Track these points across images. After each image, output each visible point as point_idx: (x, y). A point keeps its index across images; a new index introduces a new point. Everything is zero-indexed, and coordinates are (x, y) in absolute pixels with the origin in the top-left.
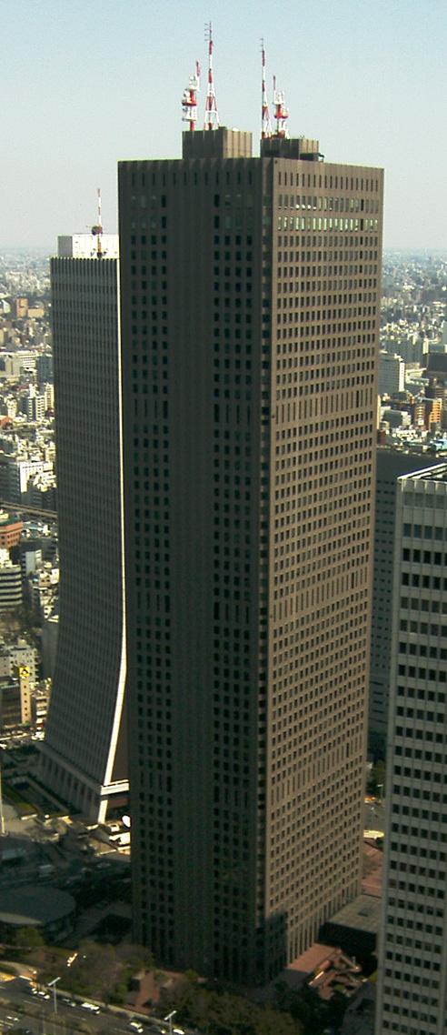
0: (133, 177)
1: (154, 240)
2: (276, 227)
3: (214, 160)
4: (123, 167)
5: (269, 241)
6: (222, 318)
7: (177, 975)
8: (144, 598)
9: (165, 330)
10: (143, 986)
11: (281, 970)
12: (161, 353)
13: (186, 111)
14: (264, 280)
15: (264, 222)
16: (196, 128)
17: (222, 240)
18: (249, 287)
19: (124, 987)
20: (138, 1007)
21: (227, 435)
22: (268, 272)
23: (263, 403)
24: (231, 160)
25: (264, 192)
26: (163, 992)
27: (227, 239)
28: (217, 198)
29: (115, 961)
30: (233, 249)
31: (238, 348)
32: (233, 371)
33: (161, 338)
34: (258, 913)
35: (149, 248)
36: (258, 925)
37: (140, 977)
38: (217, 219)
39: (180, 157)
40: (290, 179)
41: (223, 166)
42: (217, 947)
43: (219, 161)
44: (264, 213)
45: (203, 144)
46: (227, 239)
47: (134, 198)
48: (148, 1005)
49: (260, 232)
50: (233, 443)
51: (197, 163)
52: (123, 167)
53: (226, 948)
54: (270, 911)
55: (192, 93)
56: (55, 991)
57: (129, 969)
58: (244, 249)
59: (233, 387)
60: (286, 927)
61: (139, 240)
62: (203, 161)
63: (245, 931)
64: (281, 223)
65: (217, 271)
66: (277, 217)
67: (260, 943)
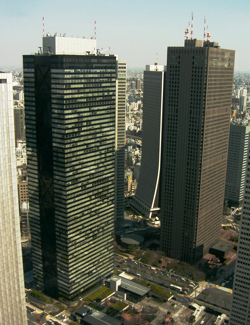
0: (172, 51)
1: (176, 67)
2: (209, 65)
3: (193, 47)
4: (169, 49)
5: (207, 68)
6: (193, 88)
7: (172, 260)
8: (168, 160)
9: (178, 90)
10: (163, 262)
11: (202, 258)
12: (177, 96)
13: (186, 34)
14: (205, 78)
15: (206, 63)
16: (188, 39)
17: (194, 68)
18: (201, 80)
19: (157, 262)
20: (161, 268)
21: (193, 118)
22: (206, 76)
23: (203, 110)
24: (197, 47)
25: (206, 56)
26: (168, 264)
27: (196, 68)
28: (193, 57)
29: (155, 255)
30: (197, 70)
31: (197, 96)
32: (196, 102)
33: (177, 92)
34: (194, 244)
35: (175, 69)
36: (194, 248)
37: (162, 260)
38: (193, 62)
39: (184, 46)
40: (213, 53)
41: (196, 48)
42: (182, 253)
43: (195, 47)
44: (206, 61)
45: (190, 43)
46: (196, 68)
47: (171, 56)
48: (164, 267)
49: (205, 66)
50: (195, 120)
51: (189, 48)
52: (169, 49)
53: (185, 254)
54: (198, 244)
55: (187, 30)
56: (140, 262)
57: (159, 258)
58: (200, 70)
59: (195, 106)
60: (203, 247)
61: (172, 67)
62: (190, 47)
63: (190, 249)
64: (210, 64)
65: (193, 75)
66: (209, 62)
67: (194, 253)
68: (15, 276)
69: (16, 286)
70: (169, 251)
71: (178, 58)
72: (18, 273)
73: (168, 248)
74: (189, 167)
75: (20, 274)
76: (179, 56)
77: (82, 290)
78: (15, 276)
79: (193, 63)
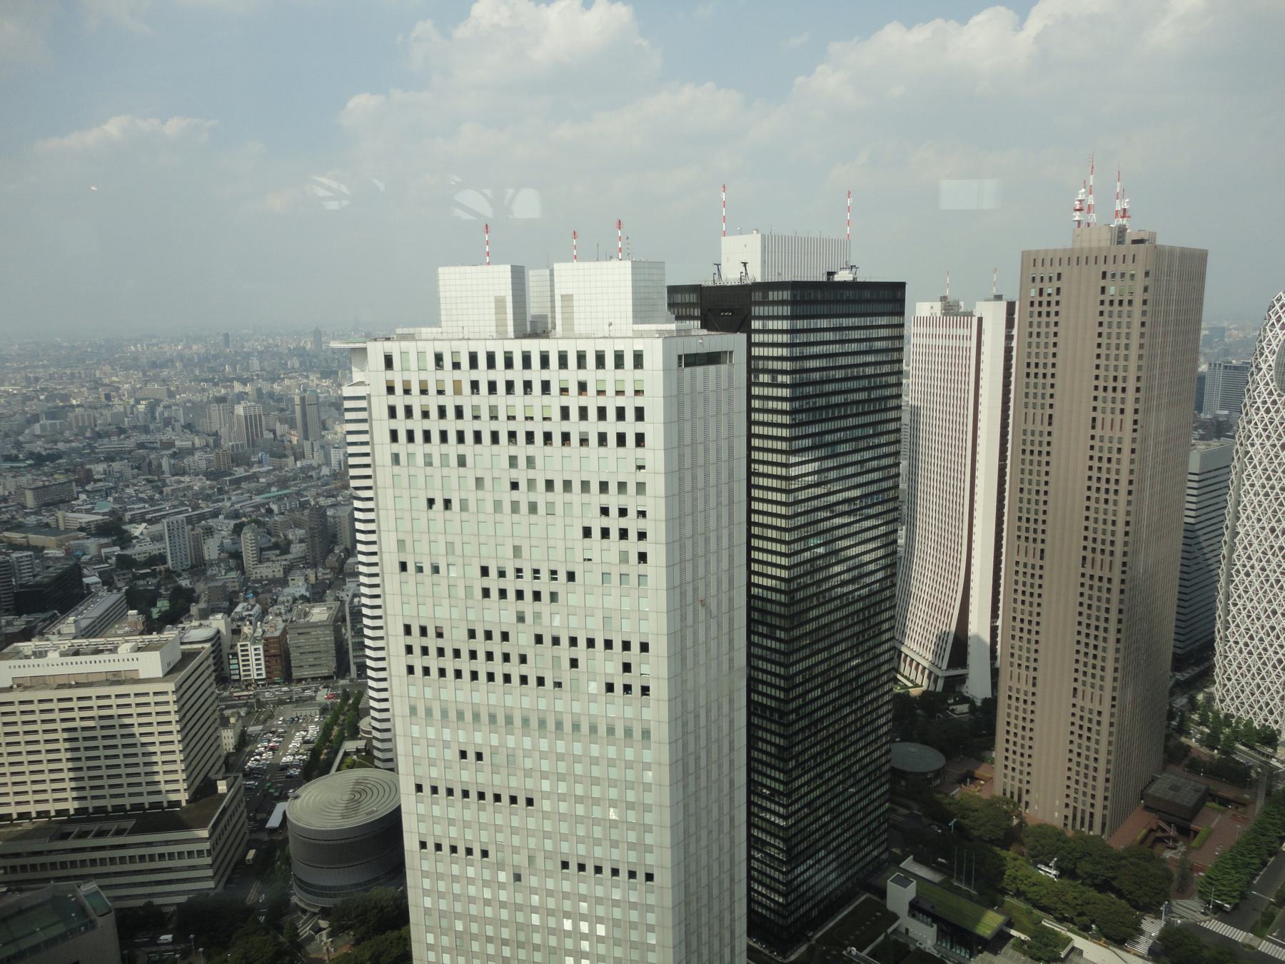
0: (1032, 261)
4: (1025, 255)
17: (1107, 303)
27: (1111, 303)
42: (1067, 805)
46: (1111, 303)
52: (1025, 255)
53: (1075, 808)
68: (727, 922)
69: (727, 951)
70: (1025, 798)
71: (1055, 278)
72: (732, 912)
73: (1020, 789)
74: (1088, 571)
75: (737, 915)
76: (1059, 275)
77: (815, 913)
78: (727, 922)
79: (1103, 289)
